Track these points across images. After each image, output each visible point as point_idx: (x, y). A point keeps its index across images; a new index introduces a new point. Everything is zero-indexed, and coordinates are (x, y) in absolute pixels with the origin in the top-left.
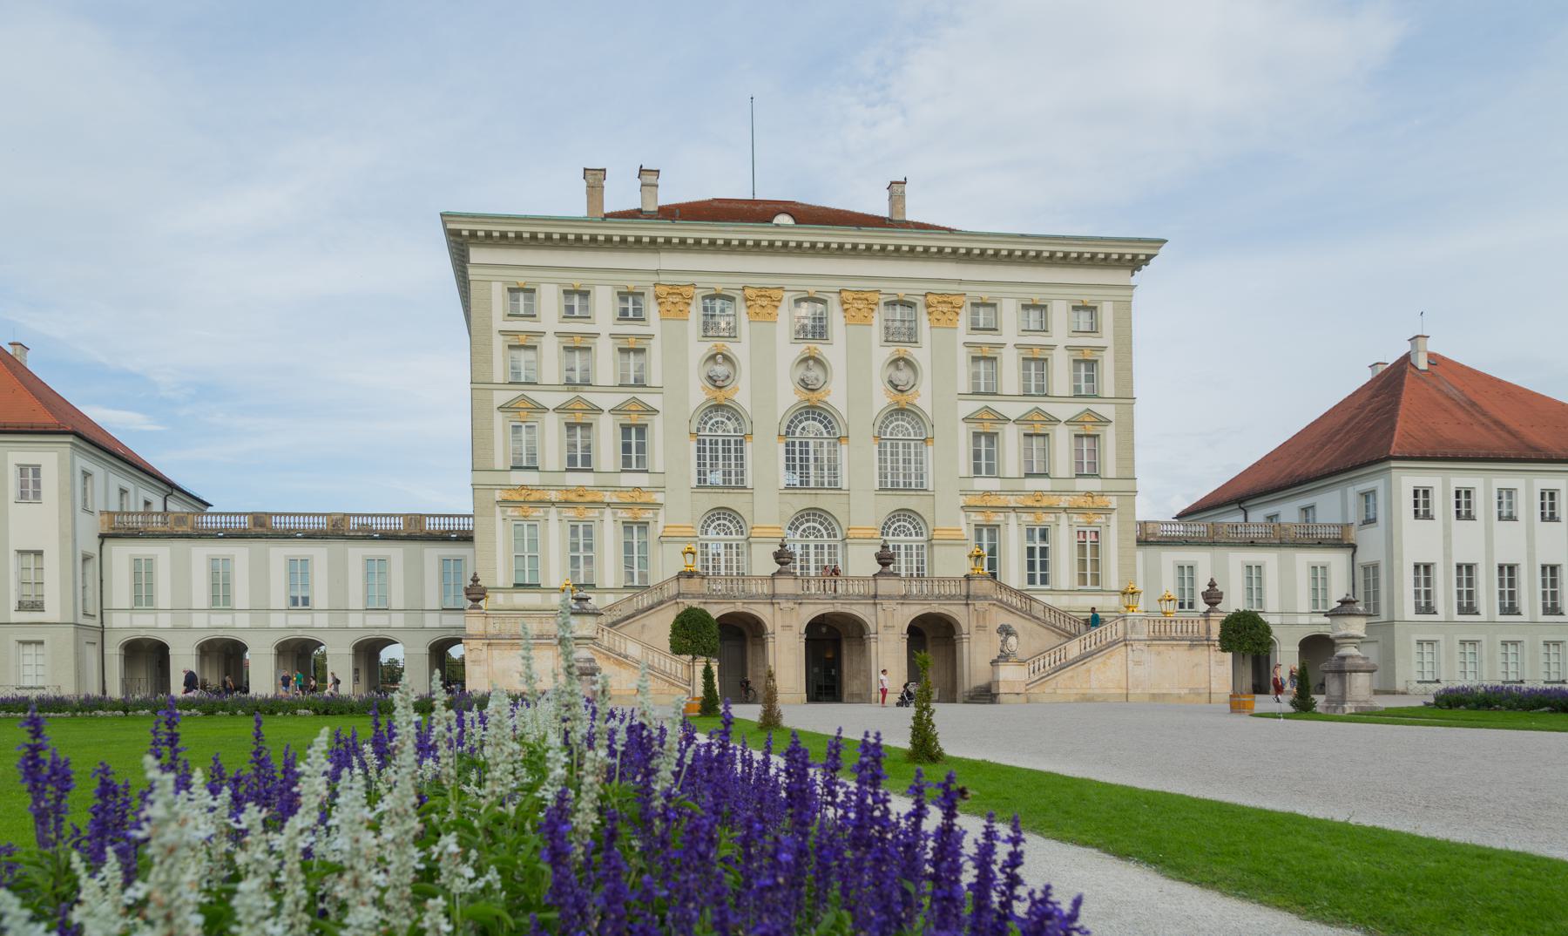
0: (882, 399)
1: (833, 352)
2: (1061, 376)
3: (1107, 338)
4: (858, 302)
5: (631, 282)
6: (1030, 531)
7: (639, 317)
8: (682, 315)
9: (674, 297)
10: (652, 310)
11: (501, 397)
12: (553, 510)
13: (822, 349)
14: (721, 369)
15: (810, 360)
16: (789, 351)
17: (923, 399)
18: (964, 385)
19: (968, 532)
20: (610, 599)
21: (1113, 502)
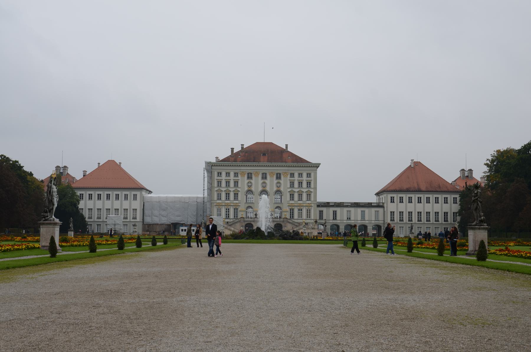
0: (275, 189)
1: (268, 181)
2: (305, 185)
3: (312, 178)
4: (272, 174)
5: (236, 171)
6: (299, 210)
7: (237, 176)
8: (244, 176)
9: (243, 174)
10: (239, 175)
11: (216, 189)
12: (223, 207)
13: (266, 181)
14: (250, 184)
15: (264, 183)
16: (260, 181)
17: (282, 189)
18: (289, 186)
19: (288, 210)
20: (232, 220)
21: (313, 205)
